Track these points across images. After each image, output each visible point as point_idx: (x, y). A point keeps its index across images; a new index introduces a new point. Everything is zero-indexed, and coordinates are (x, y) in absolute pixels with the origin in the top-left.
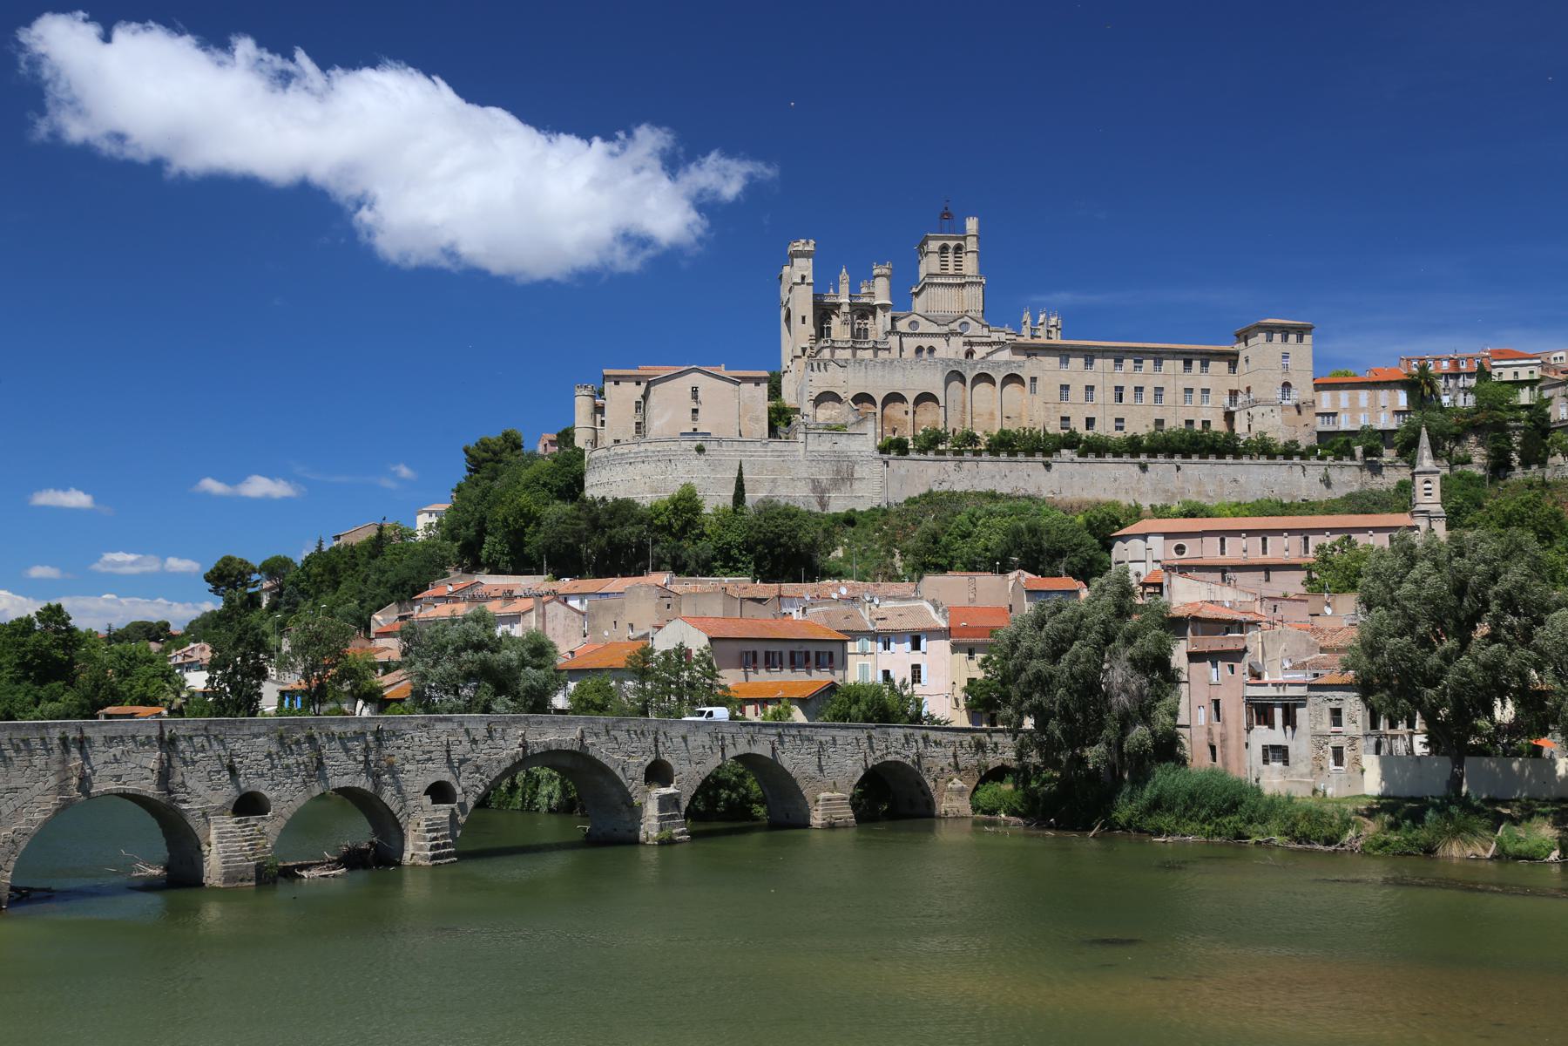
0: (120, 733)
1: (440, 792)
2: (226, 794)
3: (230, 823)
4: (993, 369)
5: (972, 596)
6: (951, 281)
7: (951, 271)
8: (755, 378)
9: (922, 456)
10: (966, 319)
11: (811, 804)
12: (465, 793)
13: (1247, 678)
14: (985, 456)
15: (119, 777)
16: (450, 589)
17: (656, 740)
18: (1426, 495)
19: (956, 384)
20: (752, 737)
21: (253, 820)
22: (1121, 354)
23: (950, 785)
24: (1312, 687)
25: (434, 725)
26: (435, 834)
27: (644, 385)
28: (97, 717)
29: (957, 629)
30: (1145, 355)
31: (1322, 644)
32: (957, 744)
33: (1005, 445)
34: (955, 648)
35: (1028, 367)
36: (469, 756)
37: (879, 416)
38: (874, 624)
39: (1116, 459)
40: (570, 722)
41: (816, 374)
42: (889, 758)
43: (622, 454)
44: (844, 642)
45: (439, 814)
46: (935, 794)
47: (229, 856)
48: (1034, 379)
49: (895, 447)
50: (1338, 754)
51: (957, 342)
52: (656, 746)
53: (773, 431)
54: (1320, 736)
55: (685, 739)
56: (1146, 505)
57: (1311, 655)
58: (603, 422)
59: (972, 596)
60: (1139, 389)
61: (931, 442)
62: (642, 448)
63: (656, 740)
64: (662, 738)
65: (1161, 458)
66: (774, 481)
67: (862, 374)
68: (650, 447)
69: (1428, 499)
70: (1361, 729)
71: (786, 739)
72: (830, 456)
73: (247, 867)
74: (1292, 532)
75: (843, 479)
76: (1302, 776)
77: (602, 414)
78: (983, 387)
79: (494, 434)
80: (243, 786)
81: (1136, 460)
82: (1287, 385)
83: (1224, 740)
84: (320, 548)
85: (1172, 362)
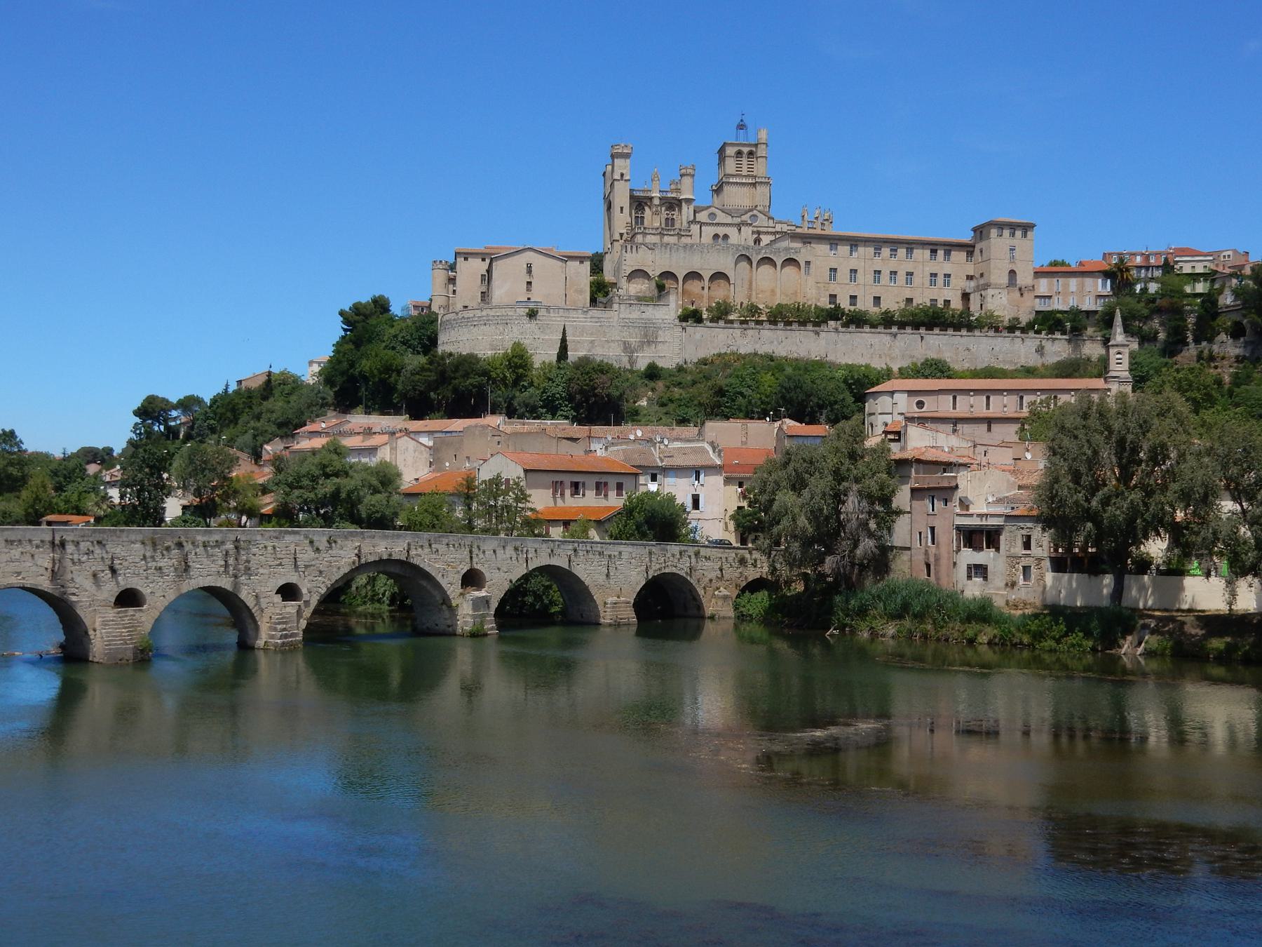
0: (19, 537)
1: (289, 592)
2: (110, 590)
3: (111, 613)
4: (775, 253)
5: (744, 439)
6: (744, 181)
7: (745, 173)
9: (714, 325)
10: (755, 212)
11: (601, 608)
12: (310, 592)
13: (958, 510)
14: (766, 325)
15: (19, 573)
16: (323, 425)
17: (471, 552)
18: (1117, 363)
19: (744, 264)
20: (552, 551)
21: (131, 610)
22: (880, 244)
23: (716, 593)
24: (1009, 518)
25: (283, 537)
26: (284, 626)
27: (488, 261)
28: (39, 524)
29: (731, 466)
30: (899, 245)
31: (1020, 483)
32: (724, 560)
33: (784, 317)
34: (728, 481)
35: (803, 253)
36: (313, 563)
37: (680, 290)
38: (662, 461)
39: (873, 330)
40: (399, 536)
41: (628, 255)
42: (667, 571)
43: (468, 318)
44: (636, 475)
45: (288, 610)
46: (704, 600)
47: (112, 640)
48: (808, 263)
49: (691, 317)
50: (1026, 569)
51: (747, 231)
52: (471, 558)
53: (593, 301)
54: (1013, 557)
55: (494, 551)
56: (895, 369)
57: (1010, 491)
58: (454, 291)
59: (744, 439)
60: (894, 273)
61: (721, 313)
62: (484, 313)
63: (471, 552)
64: (475, 551)
65: (909, 330)
66: (592, 342)
68: (491, 313)
69: (1119, 367)
70: (1045, 552)
71: (581, 553)
72: (639, 323)
73: (126, 649)
74: (1010, 391)
75: (648, 342)
76: (998, 589)
77: (454, 284)
78: (766, 269)
79: (365, 298)
80: (122, 583)
81: (888, 331)
82: (1012, 273)
83: (937, 559)
84: (226, 390)
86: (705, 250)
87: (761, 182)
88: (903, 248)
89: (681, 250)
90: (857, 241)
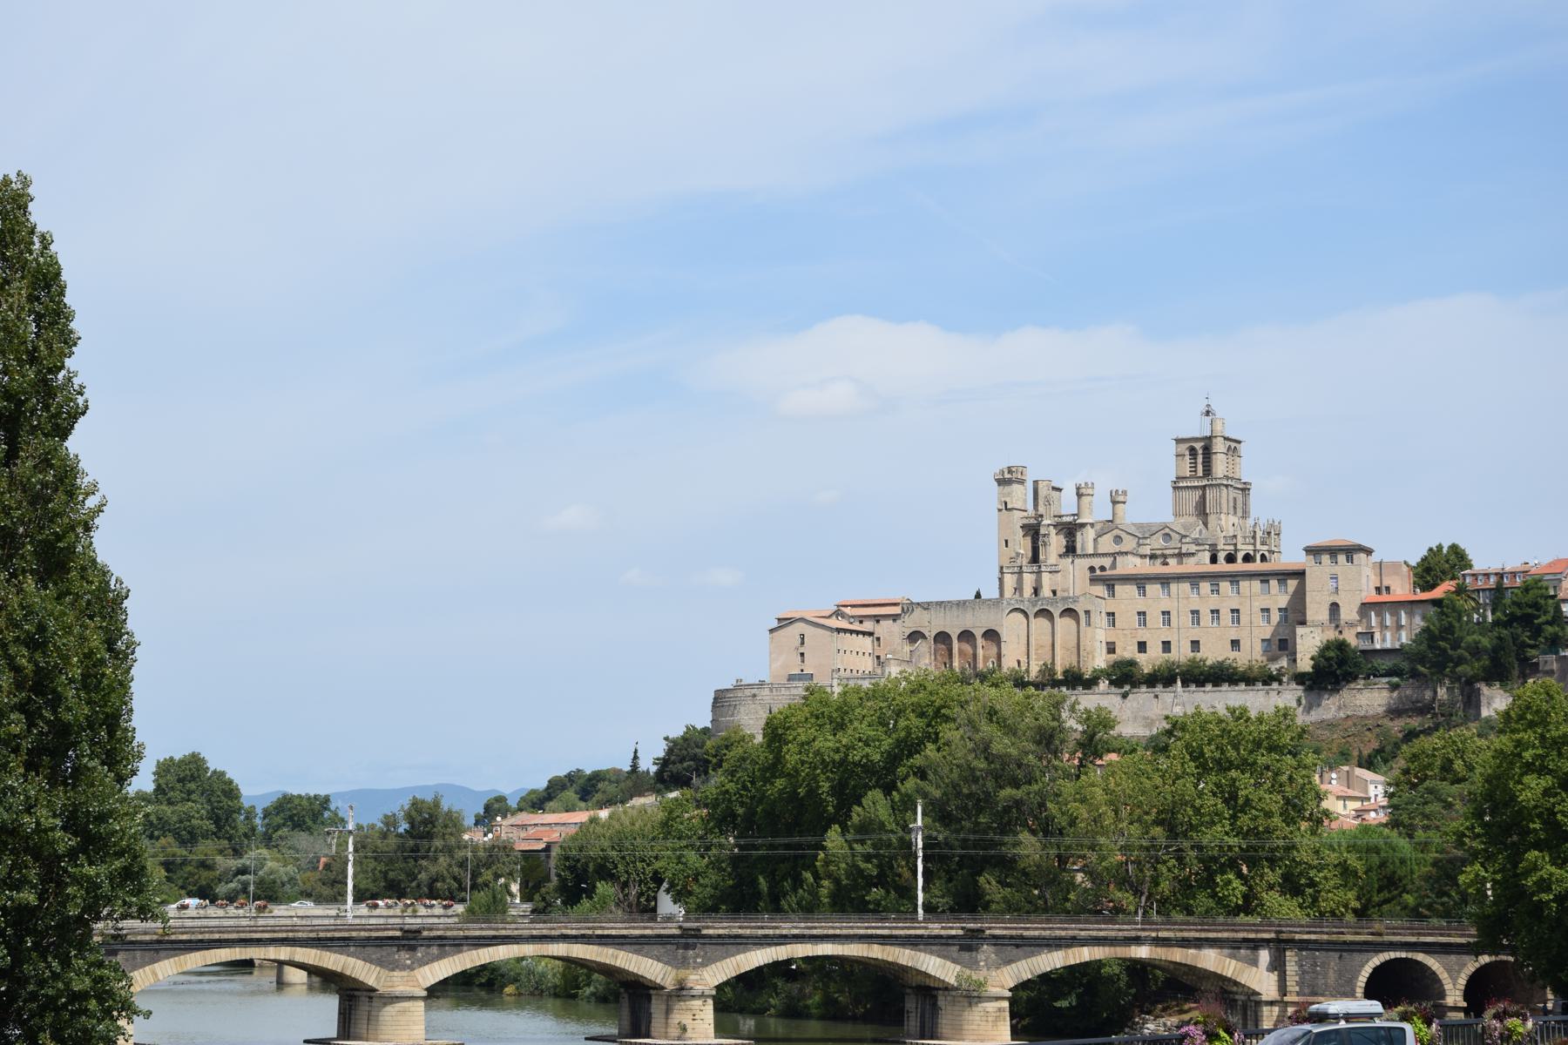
4: (1052, 605)
6: (1196, 484)
8: (875, 616)
10: (1167, 530)
19: (1020, 616)
22: (1198, 580)
60: (1215, 612)
82: (1335, 607)
85: (1248, 582)
89: (955, 607)
90: (1168, 578)
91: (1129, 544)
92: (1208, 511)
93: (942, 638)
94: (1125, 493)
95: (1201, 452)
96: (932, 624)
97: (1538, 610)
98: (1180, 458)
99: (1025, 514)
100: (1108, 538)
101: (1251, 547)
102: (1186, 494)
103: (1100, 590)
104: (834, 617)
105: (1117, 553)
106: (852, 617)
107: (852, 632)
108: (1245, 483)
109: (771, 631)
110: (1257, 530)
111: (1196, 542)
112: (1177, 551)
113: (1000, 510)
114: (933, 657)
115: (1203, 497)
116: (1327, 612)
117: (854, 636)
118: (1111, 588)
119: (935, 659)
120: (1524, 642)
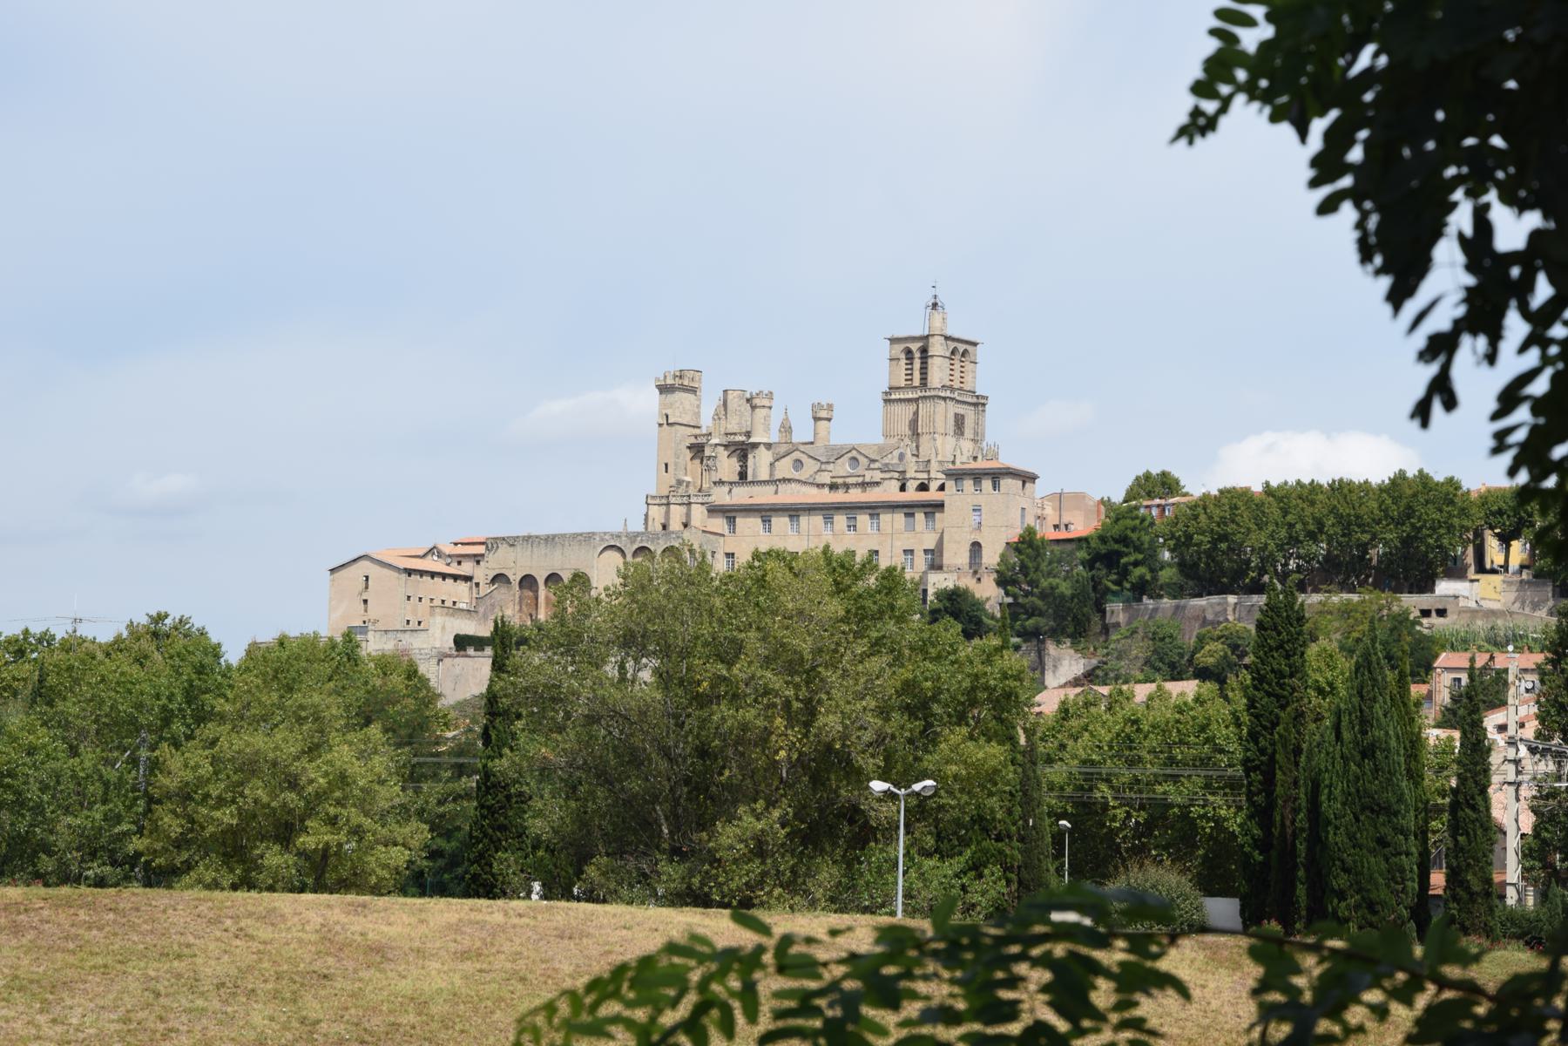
10: (854, 453)
22: (832, 512)
30: (858, 511)
67: (529, 553)
82: (976, 547)
85: (890, 515)
86: (567, 543)
87: (925, 397)
88: (865, 514)
90: (797, 510)
91: (810, 467)
92: (920, 431)
93: (528, 582)
94: (830, 407)
95: (915, 352)
96: (516, 564)
97: (1127, 546)
98: (894, 362)
99: (697, 431)
100: (788, 461)
101: (925, 476)
102: (898, 409)
103: (719, 524)
104: (429, 557)
105: (780, 480)
106: (449, 556)
107: (444, 576)
108: (978, 397)
109: (332, 571)
110: (958, 453)
111: (885, 469)
112: (860, 480)
113: (660, 425)
114: (517, 608)
115: (916, 413)
116: (967, 554)
117: (438, 580)
118: (731, 521)
119: (520, 610)
120: (1108, 590)
